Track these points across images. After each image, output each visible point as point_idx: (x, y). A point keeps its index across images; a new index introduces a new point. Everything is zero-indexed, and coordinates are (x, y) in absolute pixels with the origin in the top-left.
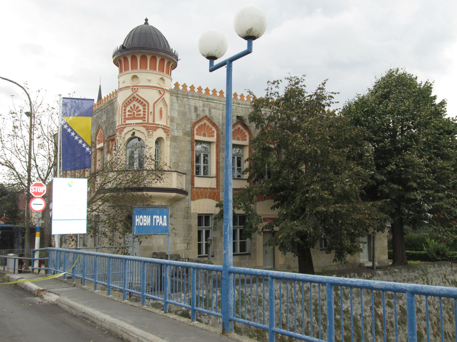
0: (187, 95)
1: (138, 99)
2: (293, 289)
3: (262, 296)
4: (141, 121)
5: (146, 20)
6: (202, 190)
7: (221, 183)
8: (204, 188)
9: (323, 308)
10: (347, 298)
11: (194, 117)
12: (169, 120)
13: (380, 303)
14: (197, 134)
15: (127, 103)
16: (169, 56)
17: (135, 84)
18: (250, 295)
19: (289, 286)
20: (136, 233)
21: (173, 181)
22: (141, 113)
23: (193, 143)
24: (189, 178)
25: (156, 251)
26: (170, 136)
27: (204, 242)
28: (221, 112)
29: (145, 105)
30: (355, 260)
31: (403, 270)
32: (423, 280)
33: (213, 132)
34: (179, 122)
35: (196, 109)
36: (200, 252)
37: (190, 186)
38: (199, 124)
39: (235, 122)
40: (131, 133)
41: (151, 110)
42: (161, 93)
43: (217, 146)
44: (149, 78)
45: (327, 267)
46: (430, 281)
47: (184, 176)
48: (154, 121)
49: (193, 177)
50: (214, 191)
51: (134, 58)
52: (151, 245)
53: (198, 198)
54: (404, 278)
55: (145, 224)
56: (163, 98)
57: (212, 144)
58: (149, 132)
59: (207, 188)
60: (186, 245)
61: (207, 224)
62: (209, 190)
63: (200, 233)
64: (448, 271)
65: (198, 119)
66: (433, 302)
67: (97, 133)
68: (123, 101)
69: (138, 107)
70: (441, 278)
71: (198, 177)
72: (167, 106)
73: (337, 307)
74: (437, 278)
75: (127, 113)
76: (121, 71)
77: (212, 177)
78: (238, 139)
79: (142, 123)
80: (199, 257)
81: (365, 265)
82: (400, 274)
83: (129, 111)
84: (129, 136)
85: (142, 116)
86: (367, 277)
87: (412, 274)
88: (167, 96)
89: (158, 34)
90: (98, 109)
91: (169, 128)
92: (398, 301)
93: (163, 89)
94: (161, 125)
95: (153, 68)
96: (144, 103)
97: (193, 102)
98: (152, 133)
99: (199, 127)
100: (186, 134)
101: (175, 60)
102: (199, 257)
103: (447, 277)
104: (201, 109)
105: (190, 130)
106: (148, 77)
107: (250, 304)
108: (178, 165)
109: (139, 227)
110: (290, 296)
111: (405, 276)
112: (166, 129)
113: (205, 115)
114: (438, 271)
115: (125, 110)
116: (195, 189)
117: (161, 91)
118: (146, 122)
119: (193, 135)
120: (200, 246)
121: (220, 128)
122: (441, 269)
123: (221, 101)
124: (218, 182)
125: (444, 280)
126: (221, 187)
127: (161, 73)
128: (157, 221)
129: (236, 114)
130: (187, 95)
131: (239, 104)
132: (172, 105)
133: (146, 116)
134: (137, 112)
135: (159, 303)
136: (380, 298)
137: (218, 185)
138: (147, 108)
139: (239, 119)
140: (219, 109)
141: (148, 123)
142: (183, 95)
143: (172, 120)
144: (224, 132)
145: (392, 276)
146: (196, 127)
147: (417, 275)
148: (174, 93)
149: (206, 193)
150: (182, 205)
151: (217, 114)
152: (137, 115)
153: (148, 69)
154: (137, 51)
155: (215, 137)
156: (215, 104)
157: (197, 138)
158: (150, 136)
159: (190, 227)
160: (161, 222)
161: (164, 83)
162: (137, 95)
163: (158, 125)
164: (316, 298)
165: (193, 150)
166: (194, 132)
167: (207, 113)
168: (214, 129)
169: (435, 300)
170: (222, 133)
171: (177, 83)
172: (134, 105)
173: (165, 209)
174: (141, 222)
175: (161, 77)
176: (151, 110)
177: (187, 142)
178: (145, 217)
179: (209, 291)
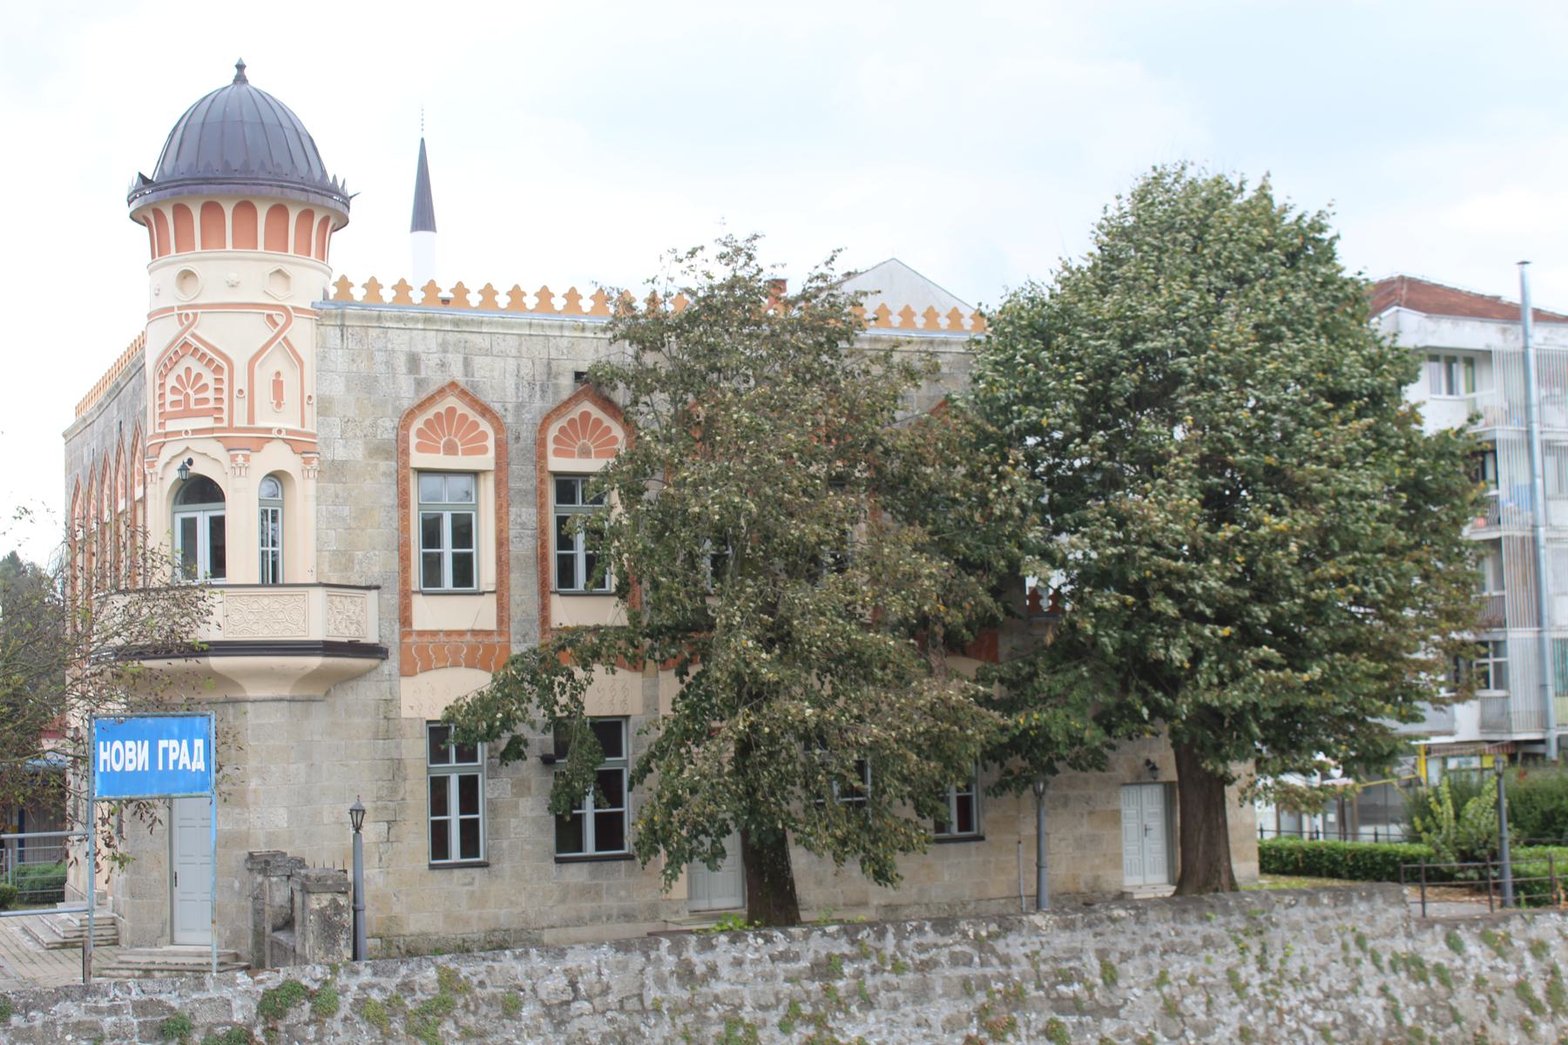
0: (379, 318)
1: (196, 350)
2: (649, 969)
3: (528, 989)
4: (207, 422)
5: (241, 67)
6: (442, 637)
7: (516, 612)
8: (449, 633)
9: (761, 1034)
10: (868, 1003)
11: (407, 394)
12: (311, 412)
13: (1012, 1025)
14: (421, 448)
15: (168, 363)
16: (302, 196)
17: (185, 300)
18: (482, 984)
19: (637, 960)
20: (101, 793)
21: (315, 618)
22: (210, 394)
23: (406, 479)
24: (393, 599)
25: (261, 848)
26: (315, 462)
27: (454, 817)
28: (511, 364)
29: (219, 369)
30: (1097, 878)
31: (1151, 915)
32: (1243, 950)
33: (484, 436)
34: (350, 414)
35: (414, 362)
36: (439, 846)
37: (397, 626)
38: (430, 414)
39: (566, 394)
40: (178, 463)
41: (241, 382)
42: (275, 324)
43: (499, 484)
44: (233, 276)
45: (964, 905)
46: (1278, 956)
47: (374, 593)
48: (251, 418)
49: (406, 595)
50: (486, 641)
51: (181, 211)
52: (244, 828)
53: (427, 668)
54: (1148, 940)
55: (130, 768)
56: (285, 339)
57: (482, 477)
58: (233, 458)
59: (461, 633)
60: (385, 826)
61: (466, 754)
62: (469, 637)
63: (438, 787)
64: (1381, 920)
65: (424, 396)
66: (1268, 1031)
67: (134, 446)
68: (157, 355)
69: (199, 376)
70: (1336, 946)
71: (424, 594)
72: (301, 363)
73: (820, 1034)
74: (1315, 945)
75: (170, 397)
76: (153, 256)
77: (483, 593)
78: (585, 453)
79: (212, 430)
80: (432, 867)
81: (1136, 897)
82: (1136, 928)
83: (174, 389)
84: (173, 475)
85: (212, 404)
86: (976, 934)
87: (1199, 928)
88: (302, 333)
89: (268, 118)
90: (134, 365)
91: (313, 436)
92: (1098, 1020)
93: (283, 308)
94: (280, 431)
95: (246, 239)
96: (217, 362)
97: (401, 341)
98: (247, 458)
99: (428, 423)
100: (377, 450)
101: (331, 203)
102: (432, 867)
103: (1370, 944)
104: (434, 360)
105: (393, 436)
106: (235, 271)
107: (475, 1013)
108: (351, 560)
109: (110, 776)
110: (635, 992)
111: (1158, 935)
112: (299, 444)
113: (448, 380)
114: (1325, 919)
115: (162, 385)
116: (414, 638)
117: (277, 315)
118: (225, 424)
119: (405, 452)
120: (439, 834)
121: (510, 419)
122: (1347, 914)
123: (511, 326)
124: (502, 607)
125: (1355, 953)
126: (514, 627)
127: (276, 255)
128: (172, 756)
129: (569, 367)
130: (379, 318)
131: (583, 329)
132: (323, 358)
133: (225, 406)
134: (196, 392)
135: (160, 1002)
136: (1015, 1010)
137: (501, 620)
138: (225, 377)
139: (587, 382)
140: (503, 355)
141: (230, 428)
142: (363, 317)
143: (325, 407)
144: (524, 435)
145: (1096, 935)
146: (418, 423)
147: (1213, 931)
148: (329, 316)
149: (457, 650)
150: (367, 693)
151: (496, 374)
152: (198, 401)
153: (229, 247)
154: (185, 189)
155: (491, 453)
156: (487, 337)
157: (418, 460)
158: (239, 470)
159: (396, 768)
160: (185, 760)
161: (288, 289)
162: (194, 335)
163: (269, 430)
164: (737, 1001)
165: (404, 504)
166: (406, 440)
167: (457, 373)
168: (485, 426)
169: (1281, 1024)
170: (518, 438)
171: (344, 278)
172: (188, 370)
173: (198, 720)
174: (118, 761)
175: (277, 266)
176: (241, 382)
177: (383, 480)
178: (130, 744)
179: (334, 969)
